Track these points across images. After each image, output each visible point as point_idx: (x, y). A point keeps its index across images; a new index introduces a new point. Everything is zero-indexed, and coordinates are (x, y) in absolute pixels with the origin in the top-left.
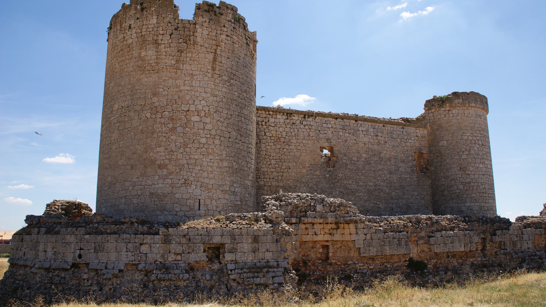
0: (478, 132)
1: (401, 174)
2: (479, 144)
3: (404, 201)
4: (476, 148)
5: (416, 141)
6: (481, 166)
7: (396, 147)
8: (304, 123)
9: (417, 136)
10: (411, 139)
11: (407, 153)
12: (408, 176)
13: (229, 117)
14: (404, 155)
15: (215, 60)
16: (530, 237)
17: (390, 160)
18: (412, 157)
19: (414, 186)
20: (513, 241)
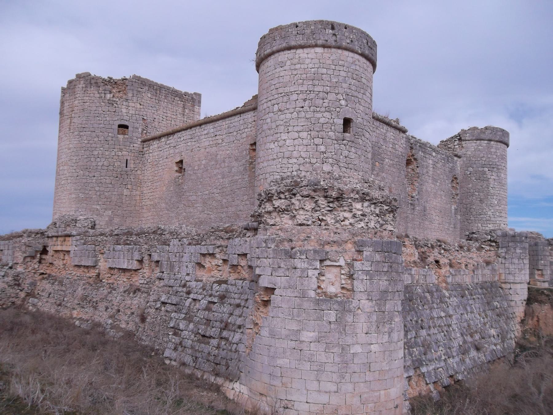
0: (274, 92)
1: (233, 176)
2: (273, 112)
3: (233, 209)
4: (269, 120)
5: (252, 128)
6: (272, 146)
7: (232, 143)
8: (168, 142)
9: (254, 121)
10: (247, 128)
11: (241, 147)
12: (240, 177)
13: (77, 161)
14: (238, 150)
15: (71, 121)
16: (192, 257)
17: (224, 162)
18: (246, 151)
19: (245, 189)
20: (171, 262)
